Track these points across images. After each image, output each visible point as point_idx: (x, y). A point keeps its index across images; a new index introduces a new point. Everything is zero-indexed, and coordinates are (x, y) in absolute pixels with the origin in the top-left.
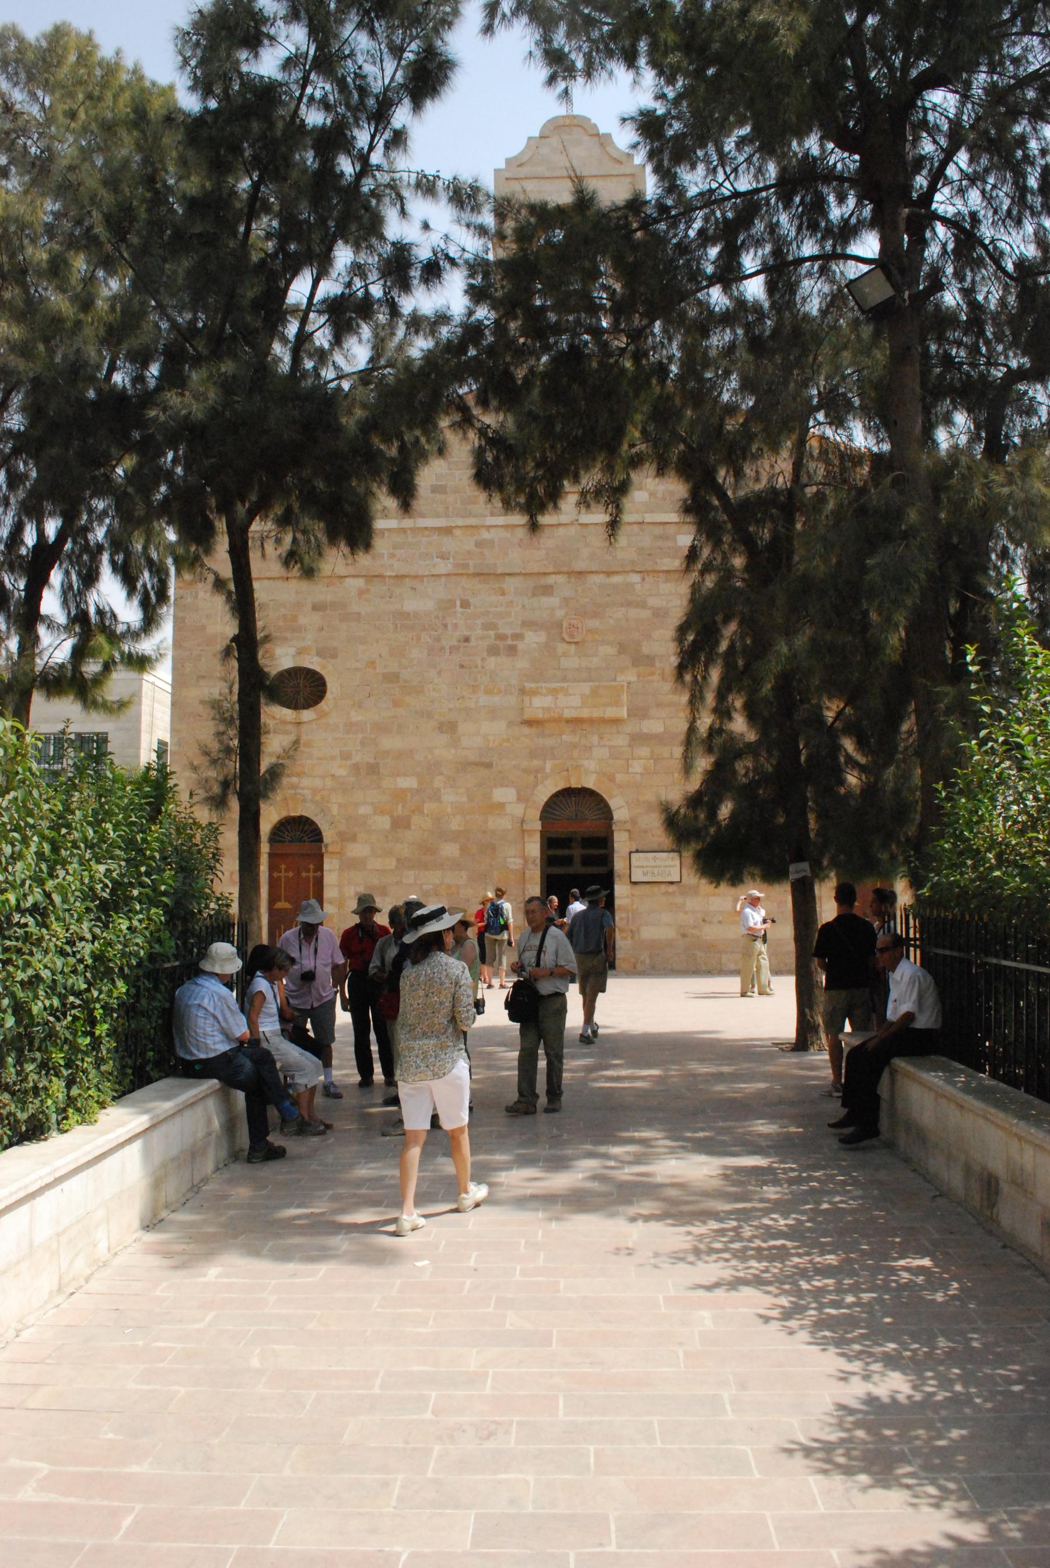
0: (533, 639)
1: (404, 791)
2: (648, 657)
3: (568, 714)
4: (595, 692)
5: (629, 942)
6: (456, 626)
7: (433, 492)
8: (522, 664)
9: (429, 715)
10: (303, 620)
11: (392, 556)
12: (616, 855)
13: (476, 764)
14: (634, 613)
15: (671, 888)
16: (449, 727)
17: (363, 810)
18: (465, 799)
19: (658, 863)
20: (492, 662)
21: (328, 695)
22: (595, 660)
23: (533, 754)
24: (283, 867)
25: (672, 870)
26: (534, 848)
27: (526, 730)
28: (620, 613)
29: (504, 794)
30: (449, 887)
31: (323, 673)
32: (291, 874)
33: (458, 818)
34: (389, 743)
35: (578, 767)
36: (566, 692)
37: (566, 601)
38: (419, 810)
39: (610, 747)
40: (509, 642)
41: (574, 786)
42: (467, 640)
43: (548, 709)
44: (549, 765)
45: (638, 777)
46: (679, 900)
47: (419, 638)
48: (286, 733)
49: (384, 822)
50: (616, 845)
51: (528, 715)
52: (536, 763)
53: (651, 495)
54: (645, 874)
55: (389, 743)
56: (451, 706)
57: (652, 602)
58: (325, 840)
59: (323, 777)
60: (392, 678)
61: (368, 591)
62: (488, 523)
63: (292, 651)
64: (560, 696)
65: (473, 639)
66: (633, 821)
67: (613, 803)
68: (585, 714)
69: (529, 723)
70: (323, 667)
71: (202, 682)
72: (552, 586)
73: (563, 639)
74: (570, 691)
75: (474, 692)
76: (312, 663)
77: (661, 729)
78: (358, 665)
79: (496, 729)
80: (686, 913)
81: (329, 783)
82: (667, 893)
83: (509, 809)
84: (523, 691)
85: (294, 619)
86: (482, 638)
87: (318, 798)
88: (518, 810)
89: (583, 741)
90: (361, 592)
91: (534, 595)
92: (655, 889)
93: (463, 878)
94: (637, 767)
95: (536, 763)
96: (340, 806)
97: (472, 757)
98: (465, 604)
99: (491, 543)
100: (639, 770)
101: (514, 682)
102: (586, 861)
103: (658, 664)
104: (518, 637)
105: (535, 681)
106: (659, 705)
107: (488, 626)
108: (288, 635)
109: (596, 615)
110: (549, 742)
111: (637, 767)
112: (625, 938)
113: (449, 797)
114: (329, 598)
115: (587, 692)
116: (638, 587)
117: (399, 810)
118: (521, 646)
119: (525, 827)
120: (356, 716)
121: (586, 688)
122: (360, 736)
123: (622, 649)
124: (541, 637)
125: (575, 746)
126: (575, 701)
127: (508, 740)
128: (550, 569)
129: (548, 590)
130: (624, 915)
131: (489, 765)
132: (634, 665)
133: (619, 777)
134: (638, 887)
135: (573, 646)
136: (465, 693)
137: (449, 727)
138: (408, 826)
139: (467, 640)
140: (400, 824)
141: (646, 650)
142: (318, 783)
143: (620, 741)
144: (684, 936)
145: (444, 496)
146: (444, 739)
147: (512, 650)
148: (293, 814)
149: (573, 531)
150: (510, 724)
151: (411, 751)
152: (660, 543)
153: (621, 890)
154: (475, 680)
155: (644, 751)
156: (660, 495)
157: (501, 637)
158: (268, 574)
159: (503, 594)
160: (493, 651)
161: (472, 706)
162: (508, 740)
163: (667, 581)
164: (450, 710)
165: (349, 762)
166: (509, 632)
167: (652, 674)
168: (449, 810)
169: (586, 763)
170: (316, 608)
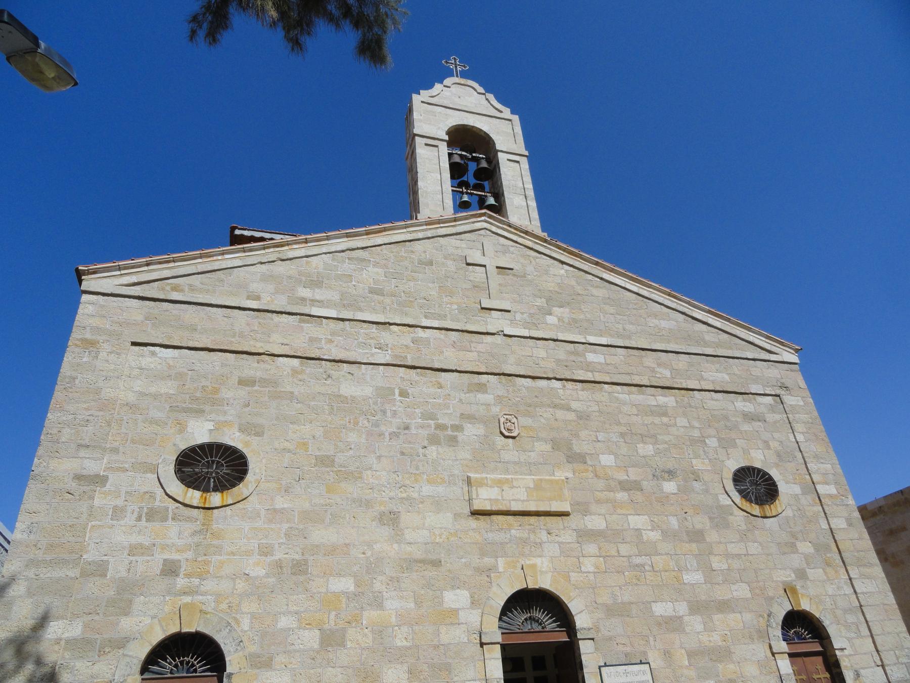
0: (472, 431)
3: (515, 507)
4: (538, 486)
6: (395, 413)
7: (371, 292)
10: (226, 393)
11: (331, 341)
12: (585, 670)
13: (423, 561)
14: (560, 414)
16: (390, 519)
17: (284, 622)
18: (412, 605)
20: (433, 451)
21: (249, 477)
27: (473, 523)
29: (457, 598)
31: (245, 451)
33: (405, 629)
34: (321, 535)
37: (499, 399)
38: (355, 620)
39: (560, 543)
40: (450, 432)
43: (497, 500)
44: (501, 563)
45: (591, 577)
47: (356, 423)
48: (189, 519)
49: (310, 638)
50: (583, 658)
51: (477, 506)
52: (488, 561)
53: (559, 320)
55: (321, 535)
56: (392, 494)
57: (574, 405)
58: (229, 669)
59: (233, 578)
60: (325, 461)
61: (302, 372)
62: (423, 325)
64: (505, 487)
68: (532, 507)
69: (476, 513)
70: (247, 444)
71: (82, 453)
72: (485, 385)
73: (501, 433)
74: (515, 484)
75: (416, 481)
76: (232, 438)
77: (603, 526)
78: (287, 444)
79: (441, 523)
81: (241, 585)
84: (469, 481)
85: (216, 391)
87: (224, 606)
88: (473, 618)
89: (532, 536)
90: (295, 372)
91: (470, 391)
94: (588, 565)
95: (487, 560)
96: (253, 616)
97: (419, 555)
99: (428, 340)
100: (592, 569)
101: (456, 472)
103: (589, 462)
104: (458, 428)
105: (476, 472)
106: (598, 501)
108: (207, 408)
111: (588, 565)
113: (393, 604)
114: (259, 374)
115: (532, 486)
117: (331, 621)
118: (461, 437)
119: (483, 641)
120: (281, 503)
121: (529, 480)
122: (286, 526)
123: (556, 445)
125: (525, 541)
126: (522, 494)
128: (483, 370)
129: (482, 388)
131: (437, 563)
133: (574, 576)
136: (407, 482)
137: (390, 519)
138: (343, 644)
140: (332, 640)
141: (576, 448)
142: (225, 586)
143: (568, 537)
145: (382, 298)
147: (453, 441)
148: (185, 630)
149: (499, 339)
150: (457, 516)
151: (347, 545)
152: (573, 358)
154: (417, 468)
155: (592, 548)
156: (566, 320)
157: (441, 427)
158: (191, 344)
159: (441, 387)
160: (434, 440)
161: (415, 495)
165: (269, 559)
167: (587, 471)
168: (393, 619)
169: (538, 561)
170: (242, 382)
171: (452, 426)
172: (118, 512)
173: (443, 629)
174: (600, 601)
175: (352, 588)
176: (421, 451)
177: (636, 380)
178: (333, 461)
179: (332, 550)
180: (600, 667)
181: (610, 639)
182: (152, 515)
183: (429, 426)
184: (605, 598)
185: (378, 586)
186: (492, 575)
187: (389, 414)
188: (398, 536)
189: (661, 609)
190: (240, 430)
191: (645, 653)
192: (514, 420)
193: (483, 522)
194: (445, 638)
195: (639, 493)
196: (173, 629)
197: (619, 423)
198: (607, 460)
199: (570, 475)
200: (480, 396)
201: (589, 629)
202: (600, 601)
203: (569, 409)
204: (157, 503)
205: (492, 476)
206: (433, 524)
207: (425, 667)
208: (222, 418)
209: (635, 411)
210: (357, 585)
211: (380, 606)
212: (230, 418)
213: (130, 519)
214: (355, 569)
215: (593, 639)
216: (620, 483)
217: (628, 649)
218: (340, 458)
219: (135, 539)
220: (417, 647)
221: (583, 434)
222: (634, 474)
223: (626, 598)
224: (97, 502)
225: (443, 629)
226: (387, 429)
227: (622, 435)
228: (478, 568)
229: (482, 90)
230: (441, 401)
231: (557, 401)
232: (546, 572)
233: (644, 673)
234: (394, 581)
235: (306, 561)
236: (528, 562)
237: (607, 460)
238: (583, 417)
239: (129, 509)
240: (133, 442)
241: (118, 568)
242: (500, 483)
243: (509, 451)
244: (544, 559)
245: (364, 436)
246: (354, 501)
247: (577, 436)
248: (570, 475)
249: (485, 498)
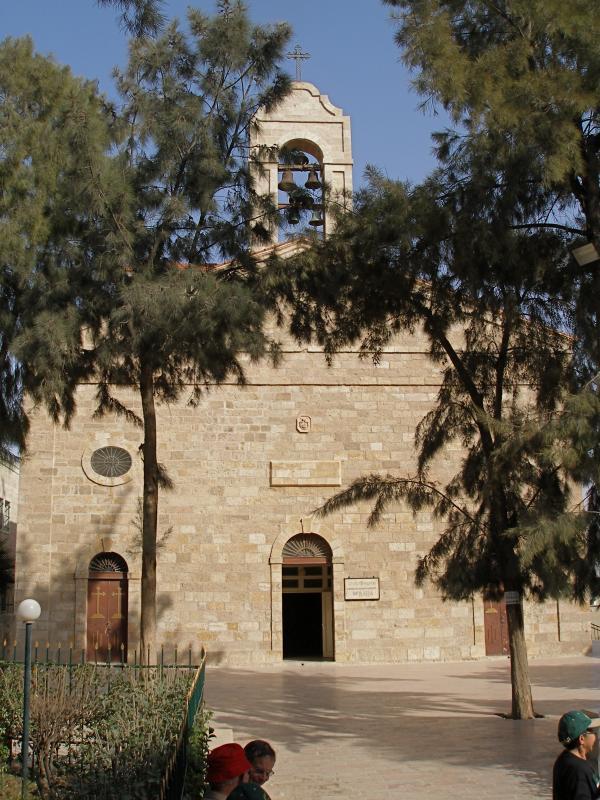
0: (276, 430)
1: (185, 536)
2: (355, 444)
3: (300, 482)
4: (319, 467)
5: (344, 641)
6: (223, 420)
8: (269, 447)
9: (204, 482)
13: (237, 517)
14: (345, 413)
15: (373, 603)
16: (218, 491)
18: (229, 542)
19: (363, 586)
22: (320, 445)
23: (276, 511)
24: (98, 588)
25: (374, 591)
26: (278, 577)
27: (271, 493)
28: (335, 413)
30: (219, 604)
31: (129, 451)
32: (104, 594)
36: (299, 466)
38: (197, 548)
40: (260, 432)
41: (305, 532)
42: (231, 430)
43: (288, 478)
46: (378, 611)
48: (102, 493)
51: (274, 483)
52: (279, 516)
54: (355, 594)
56: (220, 475)
63: (108, 436)
65: (235, 429)
66: (347, 558)
67: (332, 545)
71: (43, 456)
74: (303, 466)
80: (383, 621)
83: (259, 548)
86: (242, 429)
89: (311, 501)
91: (277, 400)
93: (227, 597)
95: (279, 516)
97: (234, 513)
98: (229, 405)
100: (350, 521)
102: (308, 584)
104: (267, 428)
105: (278, 459)
107: (246, 421)
109: (319, 414)
110: (287, 501)
112: (341, 639)
113: (218, 541)
115: (314, 467)
116: (348, 396)
117: (183, 550)
121: (314, 464)
123: (338, 437)
124: (282, 429)
126: (306, 474)
127: (259, 500)
129: (287, 397)
131: (246, 518)
132: (346, 449)
134: (350, 603)
135: (304, 435)
136: (229, 467)
137: (218, 491)
138: (189, 561)
139: (231, 430)
144: (382, 636)
146: (214, 499)
147: (262, 438)
150: (261, 488)
151: (191, 507)
153: (338, 605)
157: (255, 428)
159: (256, 398)
160: (249, 438)
161: (235, 476)
162: (259, 500)
163: (367, 392)
164: (219, 478)
166: (258, 424)
167: (359, 455)
168: (218, 549)
171: (262, 427)
172: (65, 489)
173: (247, 555)
174: (352, 541)
175: (194, 531)
176: (240, 446)
177: (414, 381)
178: (182, 456)
179: (183, 510)
182: (83, 490)
183: (246, 428)
184: (357, 540)
185: (209, 531)
187: (219, 421)
188: (222, 501)
189: (393, 547)
190: (126, 438)
191: (378, 573)
192: (308, 420)
193: (279, 492)
194: (248, 560)
195: (397, 470)
196: (100, 551)
197: (391, 418)
198: (376, 446)
199: (346, 459)
200: (285, 403)
202: (352, 541)
203: (352, 408)
204: (84, 484)
205: (287, 462)
206: (245, 493)
207: (236, 575)
208: (114, 431)
209: (407, 407)
210: (198, 530)
211: (210, 542)
212: (118, 430)
213: (71, 493)
214: (196, 520)
216: (383, 463)
218: (187, 453)
219: (75, 504)
220: (232, 564)
221: (361, 428)
222: (395, 456)
223: (371, 541)
224: (54, 484)
225: (247, 555)
226: (217, 432)
227: (392, 427)
229: (315, 91)
230: (255, 409)
231: (343, 403)
234: (220, 529)
235: (167, 516)
237: (376, 446)
238: (363, 414)
239: (70, 487)
240: (67, 448)
241: (69, 518)
242: (292, 467)
243: (303, 444)
245: (202, 437)
246: (195, 480)
247: (356, 429)
248: (346, 459)
249: (280, 476)
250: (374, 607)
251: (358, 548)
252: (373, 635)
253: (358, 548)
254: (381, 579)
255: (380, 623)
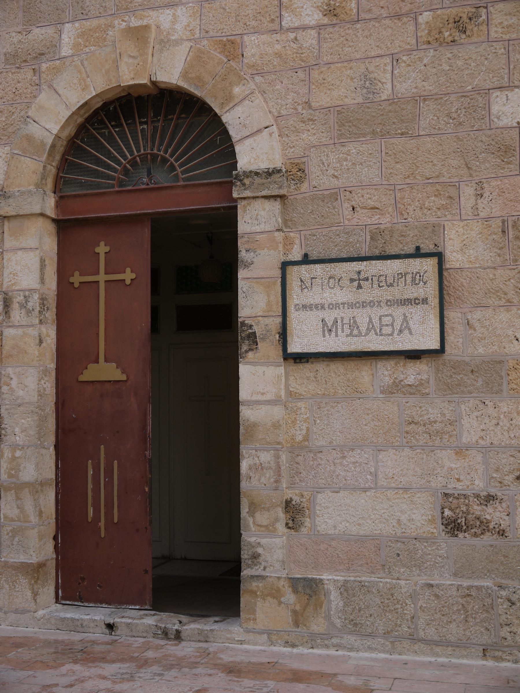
12: (242, 274)
15: (413, 373)
35: (139, 35)
45: (309, 39)
46: (436, 409)
54: (328, 329)
80: (460, 452)
82: (396, 388)
92: (364, 374)
130: (266, 457)
134: (306, 370)
144: (453, 527)
153: (258, 380)
174: (321, 99)
180: (285, 265)
181: (334, 196)
184: (341, 91)
186: (44, 66)
191: (437, 229)
201: (269, 173)
215: (282, 197)
217: (385, 221)
223: (405, 88)
228: (15, 56)
232: (178, 42)
233: (417, 279)
236: (135, 23)
244: (180, 11)
250: (416, 390)
251: (348, 124)
252: (419, 516)
253: (348, 124)
254: (454, 259)
255: (447, 459)
